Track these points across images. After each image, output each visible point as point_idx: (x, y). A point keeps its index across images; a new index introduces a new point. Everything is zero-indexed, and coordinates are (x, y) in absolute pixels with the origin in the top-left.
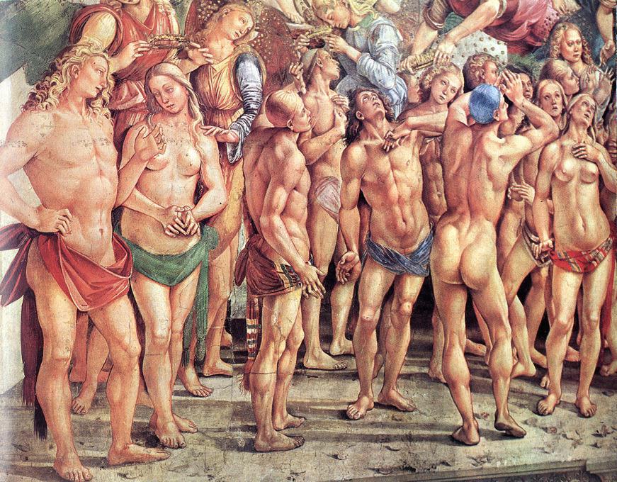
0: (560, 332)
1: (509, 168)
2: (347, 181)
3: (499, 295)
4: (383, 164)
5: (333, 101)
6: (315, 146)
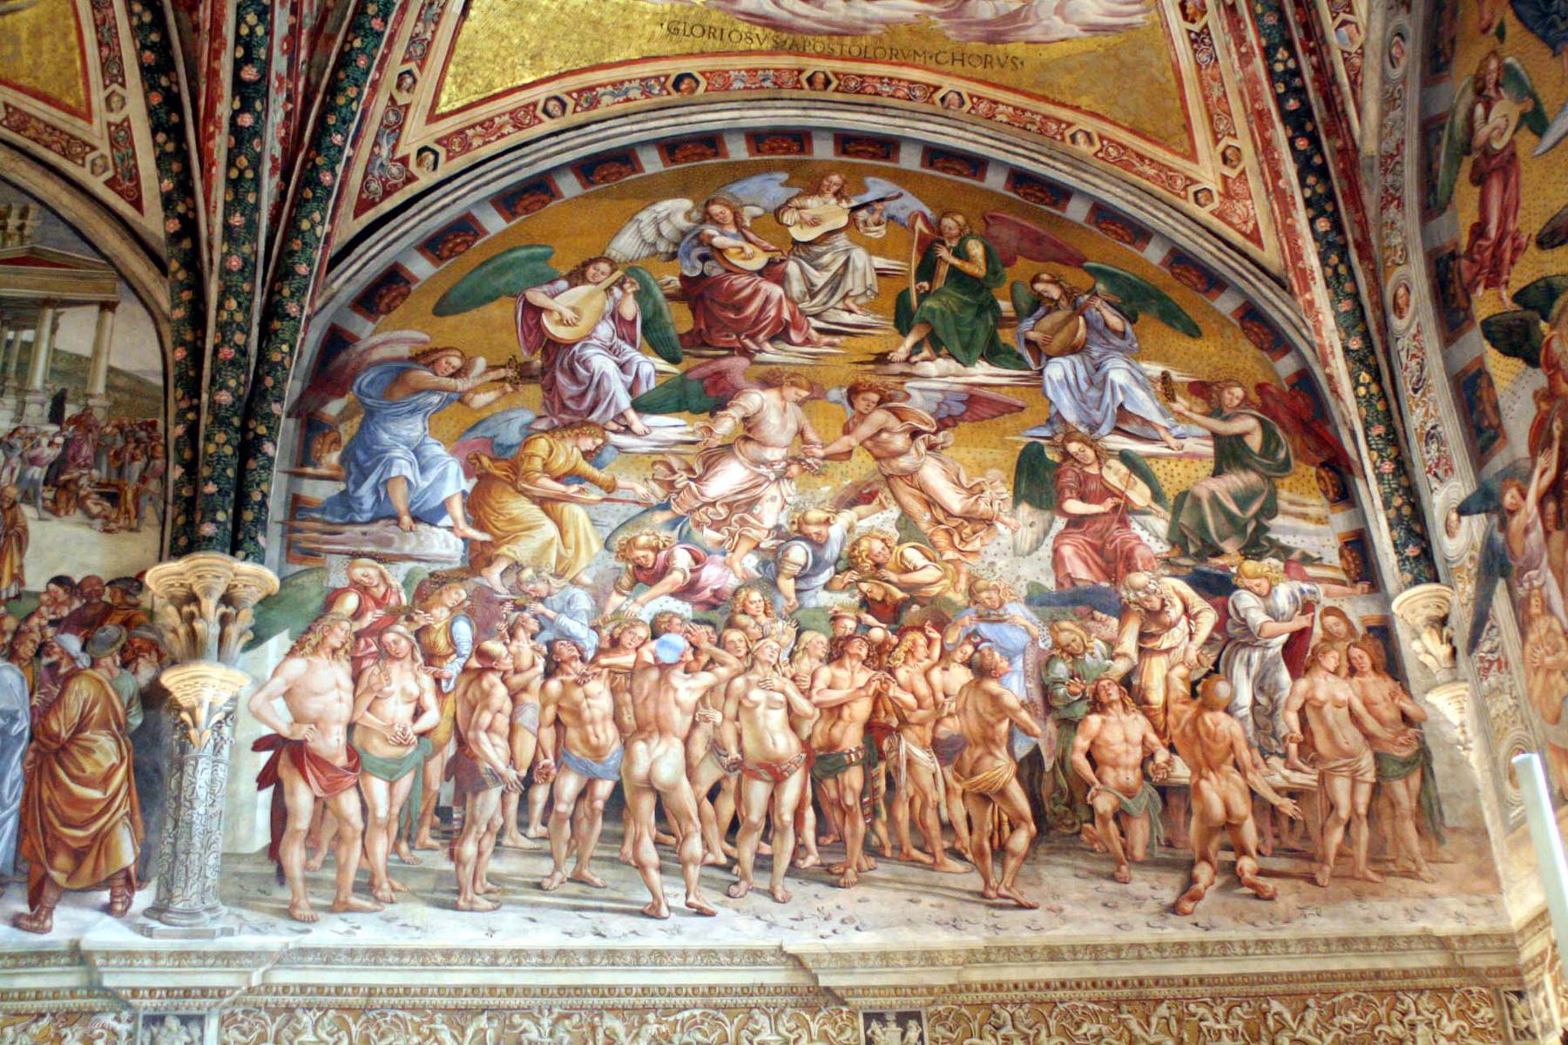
0: (752, 828)
1: (697, 696)
2: (544, 706)
3: (687, 797)
4: (578, 694)
5: (533, 649)
6: (516, 680)
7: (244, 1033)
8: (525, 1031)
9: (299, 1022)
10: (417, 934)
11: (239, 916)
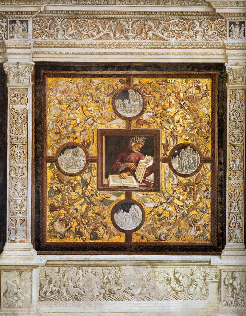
7: (40, 26)
8: (124, 26)
9: (56, 22)
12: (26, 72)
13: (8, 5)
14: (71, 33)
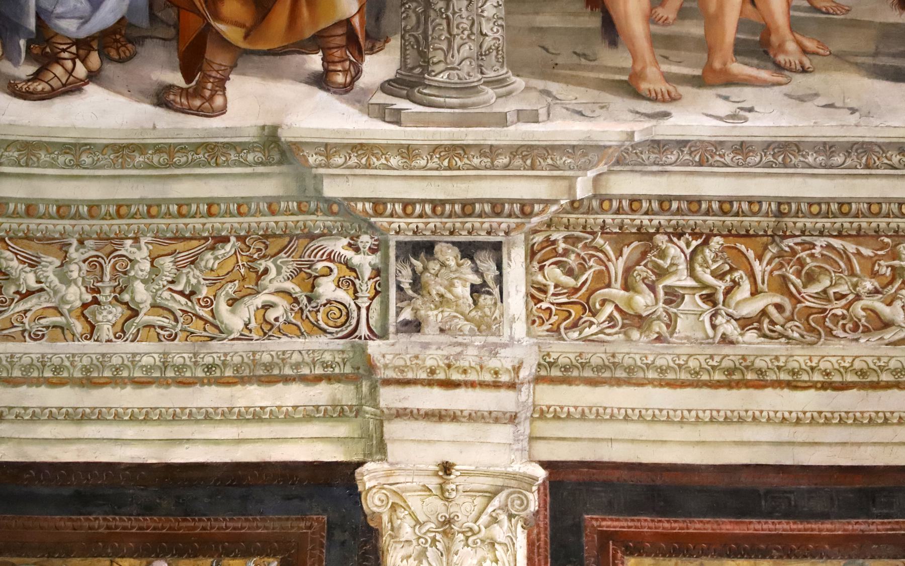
7: (570, 272)
9: (662, 254)
10: (853, 119)
11: (547, 93)
12: (495, 520)
13: (391, 168)
14: (752, 308)
